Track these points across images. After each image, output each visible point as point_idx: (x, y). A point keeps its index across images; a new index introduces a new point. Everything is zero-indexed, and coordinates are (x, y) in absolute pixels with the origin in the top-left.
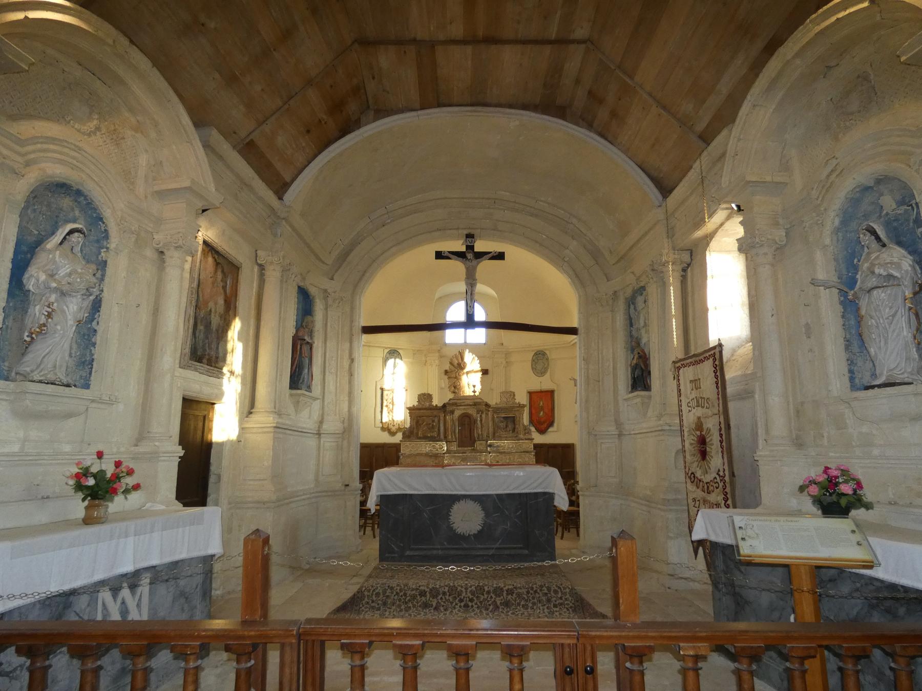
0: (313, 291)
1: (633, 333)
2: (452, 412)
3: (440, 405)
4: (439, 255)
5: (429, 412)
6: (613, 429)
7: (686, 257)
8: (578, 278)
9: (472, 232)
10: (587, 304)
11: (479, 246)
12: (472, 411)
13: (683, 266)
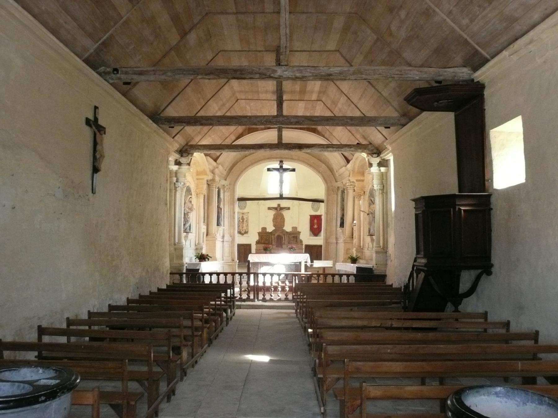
4: (269, 170)
6: (334, 241)
11: (285, 166)
12: (281, 234)
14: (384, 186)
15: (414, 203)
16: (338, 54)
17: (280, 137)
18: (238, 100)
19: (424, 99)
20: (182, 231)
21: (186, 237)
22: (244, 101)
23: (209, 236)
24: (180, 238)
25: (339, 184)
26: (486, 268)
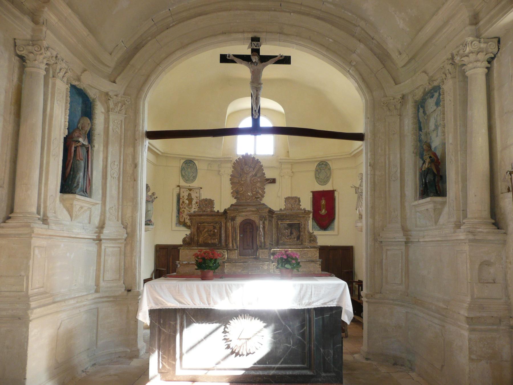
0: (92, 94)
1: (423, 137)
2: (233, 219)
3: (222, 211)
4: (224, 59)
5: (209, 219)
6: (400, 237)
7: (493, 47)
8: (366, 82)
9: (258, 35)
10: (376, 108)
11: (265, 50)
12: (255, 218)
13: (488, 56)
23: (10, 223)
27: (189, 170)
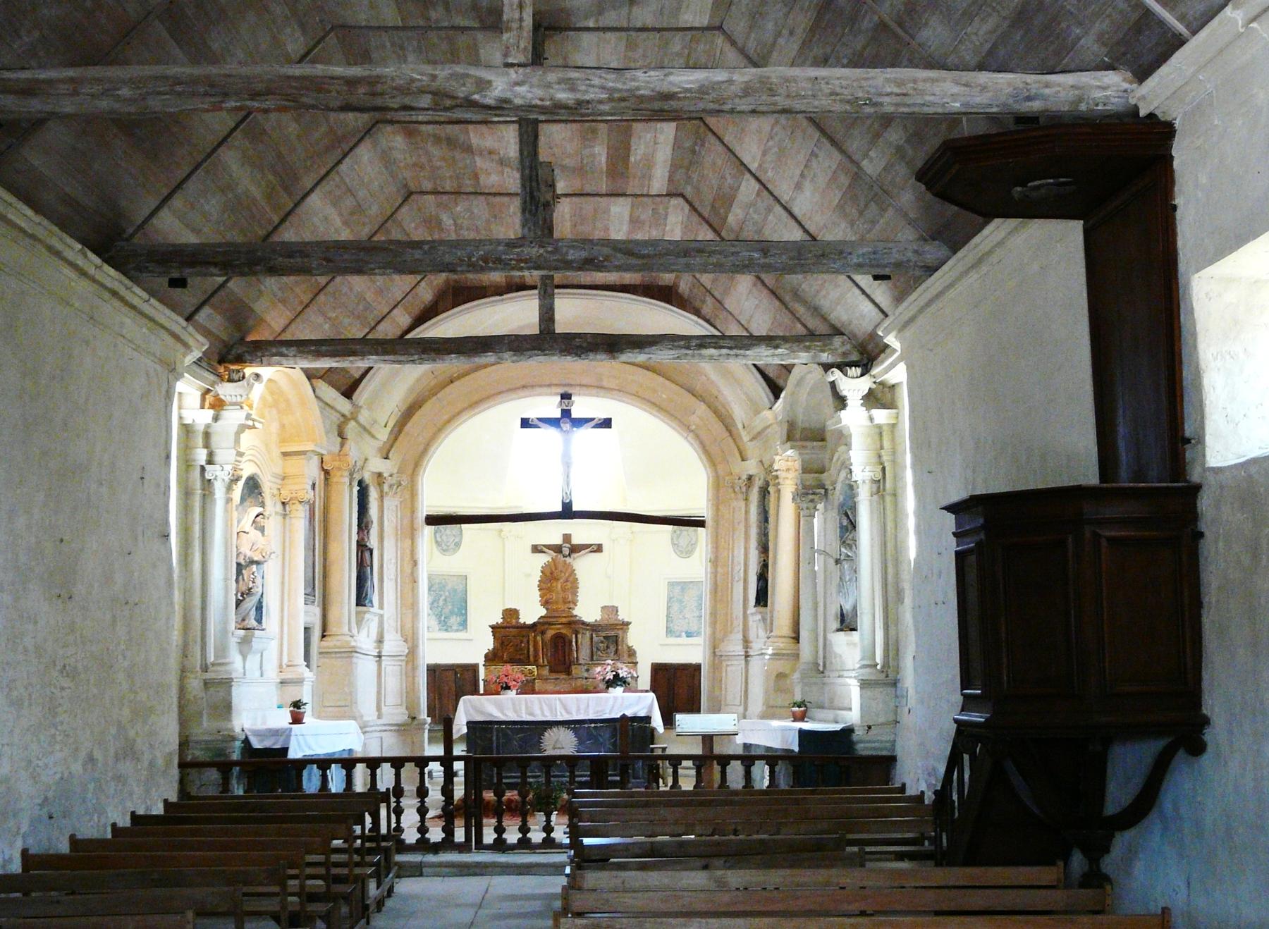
2: (543, 633)
4: (525, 423)
6: (739, 649)
9: (570, 391)
14: (884, 469)
15: (950, 519)
16: (720, 40)
17: (547, 316)
18: (411, 194)
19: (976, 176)
20: (232, 625)
21: (245, 643)
22: (431, 198)
24: (222, 650)
25: (751, 467)
26: (1186, 733)
27: (448, 532)
